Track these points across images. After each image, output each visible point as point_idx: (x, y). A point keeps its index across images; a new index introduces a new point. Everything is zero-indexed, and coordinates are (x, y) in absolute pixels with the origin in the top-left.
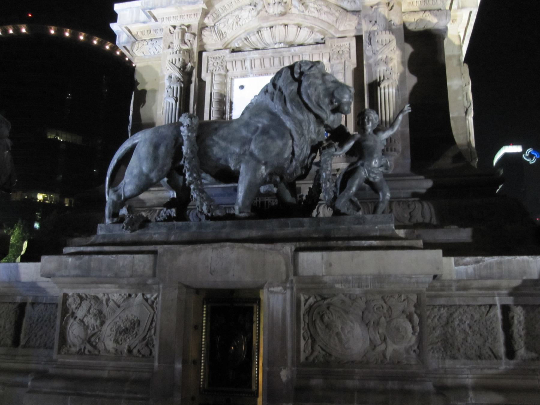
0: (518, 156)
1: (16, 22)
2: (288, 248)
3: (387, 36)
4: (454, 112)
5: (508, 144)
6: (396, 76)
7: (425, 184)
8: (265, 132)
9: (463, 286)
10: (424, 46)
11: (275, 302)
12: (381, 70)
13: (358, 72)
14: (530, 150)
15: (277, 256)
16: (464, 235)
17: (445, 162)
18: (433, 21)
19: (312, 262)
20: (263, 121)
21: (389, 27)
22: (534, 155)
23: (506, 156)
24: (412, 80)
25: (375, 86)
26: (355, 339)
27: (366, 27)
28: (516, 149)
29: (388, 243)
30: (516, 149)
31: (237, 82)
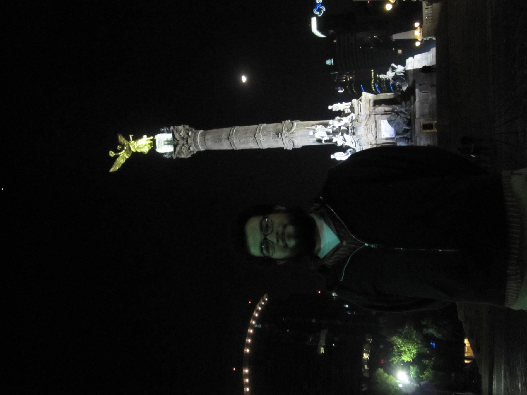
0: (319, 20)
1: (241, 376)
2: (416, 119)
3: (376, 109)
4: (388, 98)
5: (310, 28)
6: (384, 108)
7: (404, 102)
8: (399, 125)
9: (420, 98)
10: (377, 103)
11: (422, 121)
12: (383, 110)
13: (382, 114)
14: (315, 11)
15: (417, 121)
16: (412, 98)
17: (399, 99)
18: (372, 102)
19: (417, 116)
20: (397, 126)
21: (375, 109)
22: (319, 8)
23: (319, 29)
24: (383, 105)
25: (385, 111)
26: (426, 111)
27: (374, 113)
28: (314, 22)
29: (414, 107)
30: (314, 22)
31: (383, 137)
